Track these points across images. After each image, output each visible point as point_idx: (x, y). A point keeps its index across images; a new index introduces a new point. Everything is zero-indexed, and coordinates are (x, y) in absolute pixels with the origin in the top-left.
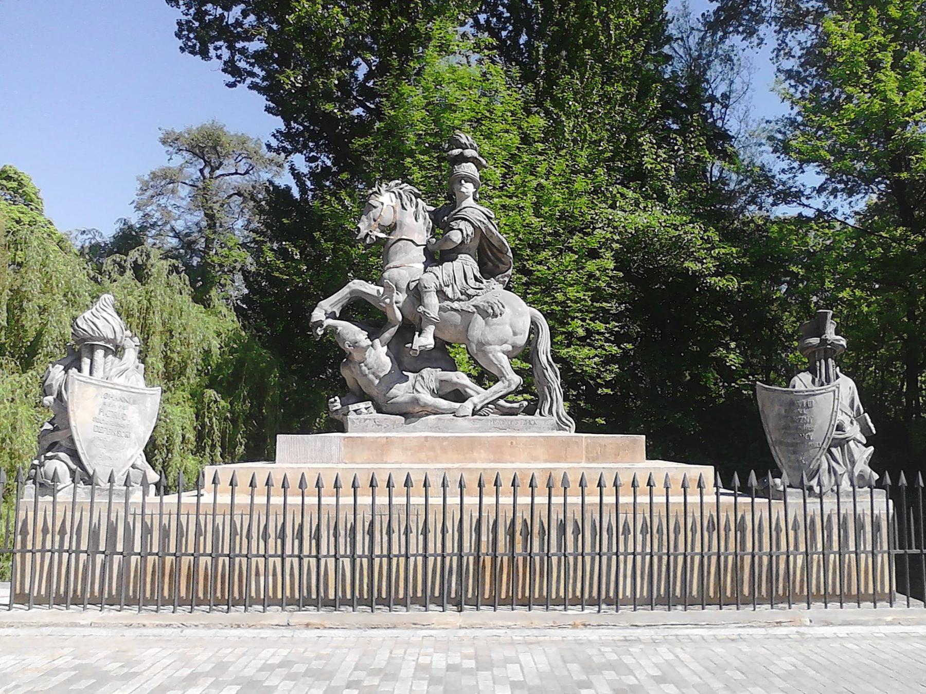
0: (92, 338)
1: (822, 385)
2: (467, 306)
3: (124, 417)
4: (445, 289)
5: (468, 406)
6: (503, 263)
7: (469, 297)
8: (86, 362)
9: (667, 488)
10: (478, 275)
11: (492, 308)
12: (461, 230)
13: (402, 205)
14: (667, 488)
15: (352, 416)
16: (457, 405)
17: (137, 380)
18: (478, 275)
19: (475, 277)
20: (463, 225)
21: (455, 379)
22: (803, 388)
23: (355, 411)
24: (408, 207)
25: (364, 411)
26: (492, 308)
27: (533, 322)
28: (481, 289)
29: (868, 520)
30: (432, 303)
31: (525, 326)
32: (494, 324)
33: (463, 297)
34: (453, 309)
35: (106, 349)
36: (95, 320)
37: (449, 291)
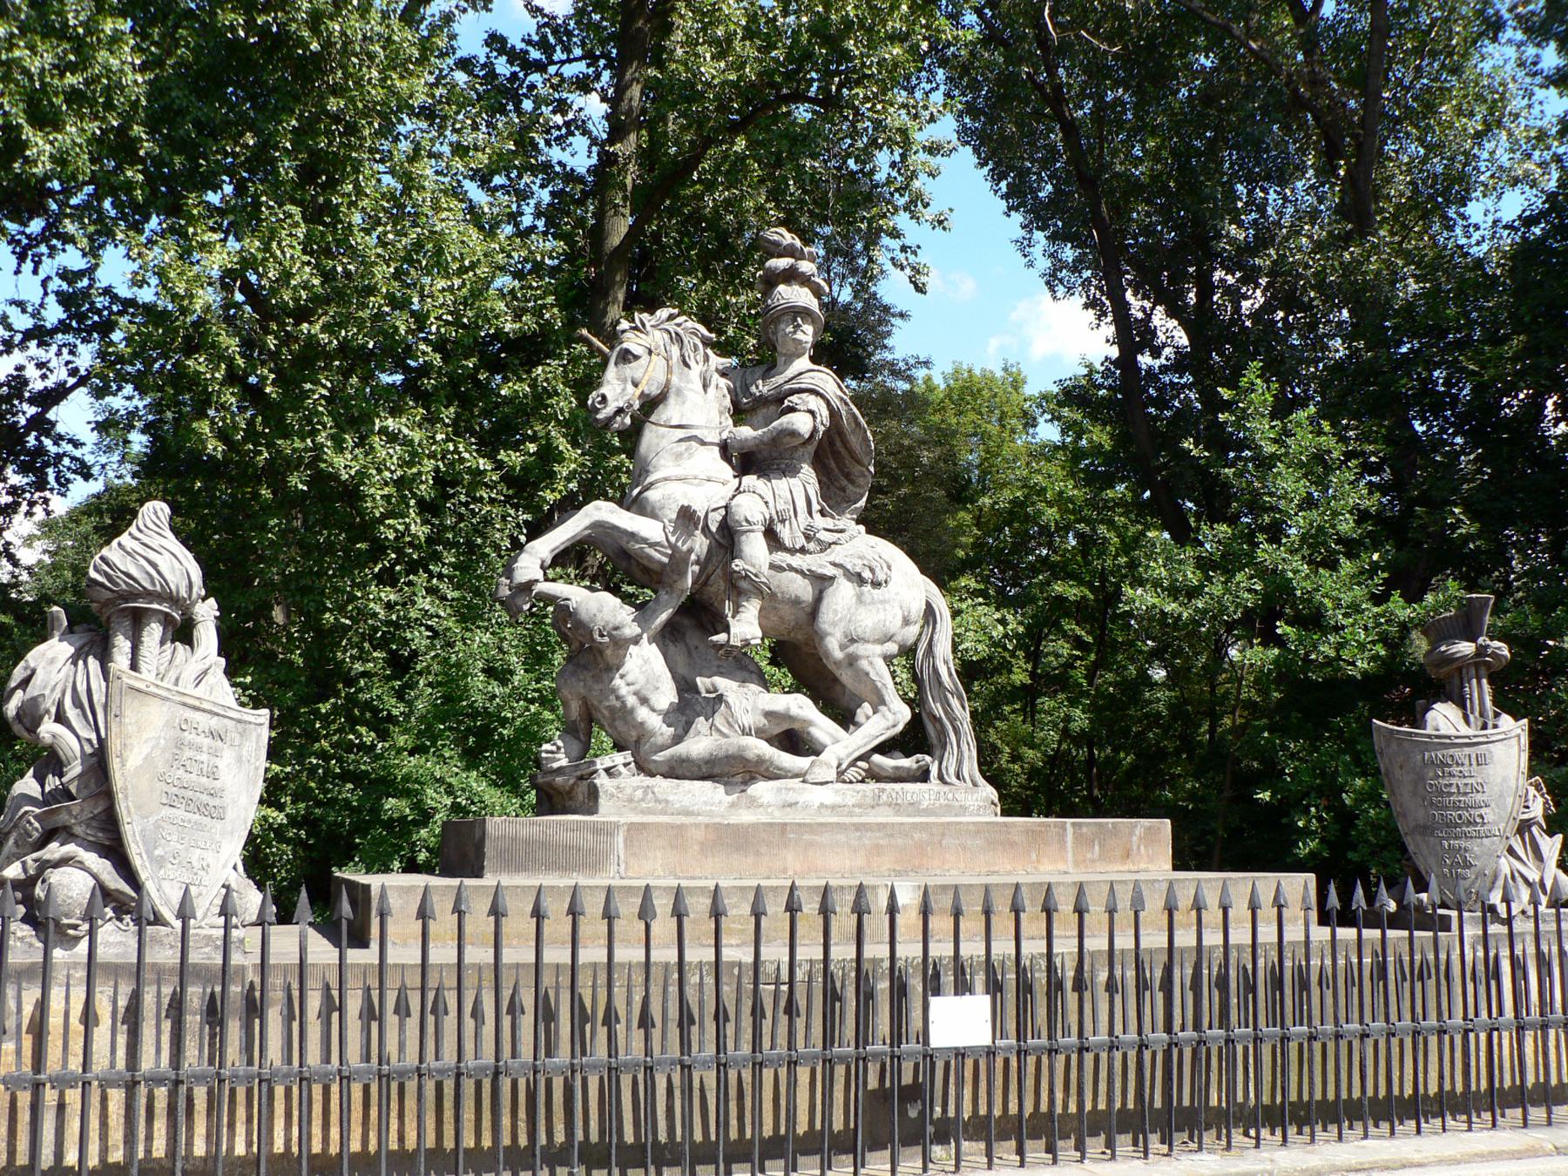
0: (134, 596)
1: (1484, 727)
2: (818, 563)
3: (213, 775)
4: (779, 528)
6: (852, 482)
7: (825, 547)
8: (122, 645)
9: (1280, 907)
11: (872, 570)
12: (812, 412)
13: (683, 356)
14: (1280, 907)
15: (602, 781)
17: (221, 691)
20: (814, 402)
21: (795, 711)
22: (1453, 732)
23: (607, 770)
24: (692, 363)
25: (621, 768)
26: (872, 570)
28: (842, 531)
29: (1041, 977)
30: (755, 553)
31: (917, 609)
32: (873, 602)
33: (811, 546)
34: (791, 568)
35: (167, 620)
36: (152, 555)
37: (784, 533)
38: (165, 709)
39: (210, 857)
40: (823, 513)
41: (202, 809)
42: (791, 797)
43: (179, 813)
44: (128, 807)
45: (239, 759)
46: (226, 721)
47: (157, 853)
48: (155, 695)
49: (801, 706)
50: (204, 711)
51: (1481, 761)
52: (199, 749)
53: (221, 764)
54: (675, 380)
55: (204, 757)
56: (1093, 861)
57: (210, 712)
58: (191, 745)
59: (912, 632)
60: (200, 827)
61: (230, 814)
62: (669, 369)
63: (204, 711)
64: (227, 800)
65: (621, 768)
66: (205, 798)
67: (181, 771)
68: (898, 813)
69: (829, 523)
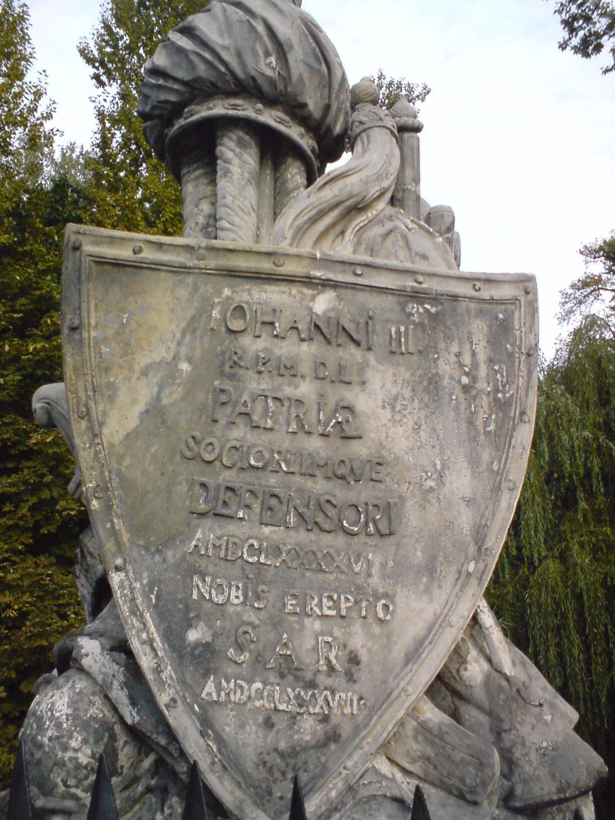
38: (183, 293)
39: (358, 641)
41: (316, 515)
44: (114, 533)
45: (430, 387)
46: (363, 297)
47: (193, 636)
48: (155, 267)
50: (289, 280)
53: (362, 402)
55: (306, 389)
57: (308, 281)
58: (262, 364)
61: (413, 518)
63: (289, 280)
66: (319, 486)
67: (239, 433)
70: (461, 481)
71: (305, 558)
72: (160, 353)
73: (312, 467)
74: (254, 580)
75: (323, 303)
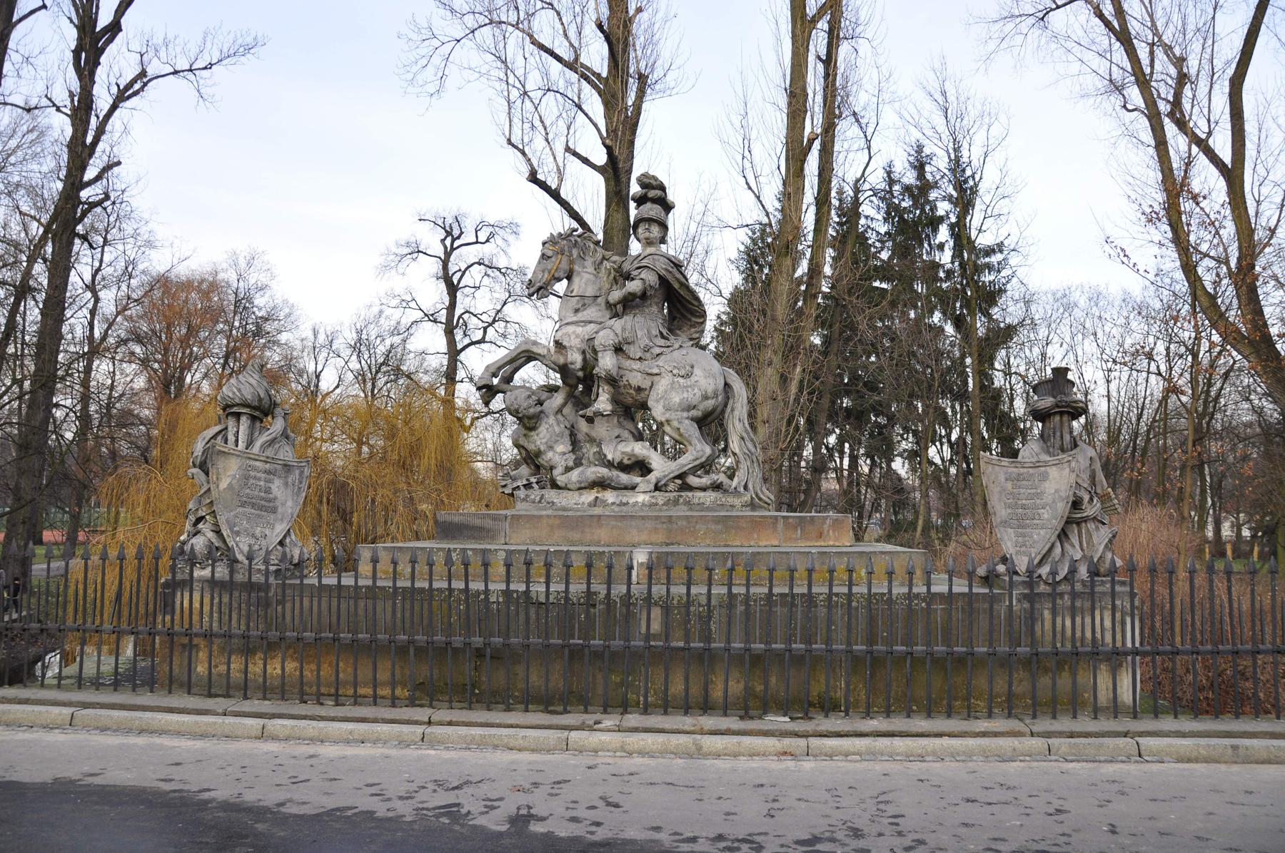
3: (268, 491)
5: (652, 477)
10: (665, 332)
16: (638, 479)
18: (665, 332)
19: (661, 333)
25: (535, 485)
27: (726, 385)
33: (648, 355)
40: (663, 337)
41: (261, 508)
42: (624, 500)
43: (249, 510)
45: (286, 484)
49: (640, 449)
51: (1044, 477)
52: (259, 479)
54: (576, 267)
56: (796, 539)
58: (255, 477)
59: (710, 404)
60: (259, 516)
62: (571, 262)
64: (278, 503)
65: (535, 485)
68: (691, 509)
69: (662, 342)
70: (290, 503)
71: (259, 516)
72: (232, 473)
73: (262, 499)
74: (249, 519)
75: (268, 466)
